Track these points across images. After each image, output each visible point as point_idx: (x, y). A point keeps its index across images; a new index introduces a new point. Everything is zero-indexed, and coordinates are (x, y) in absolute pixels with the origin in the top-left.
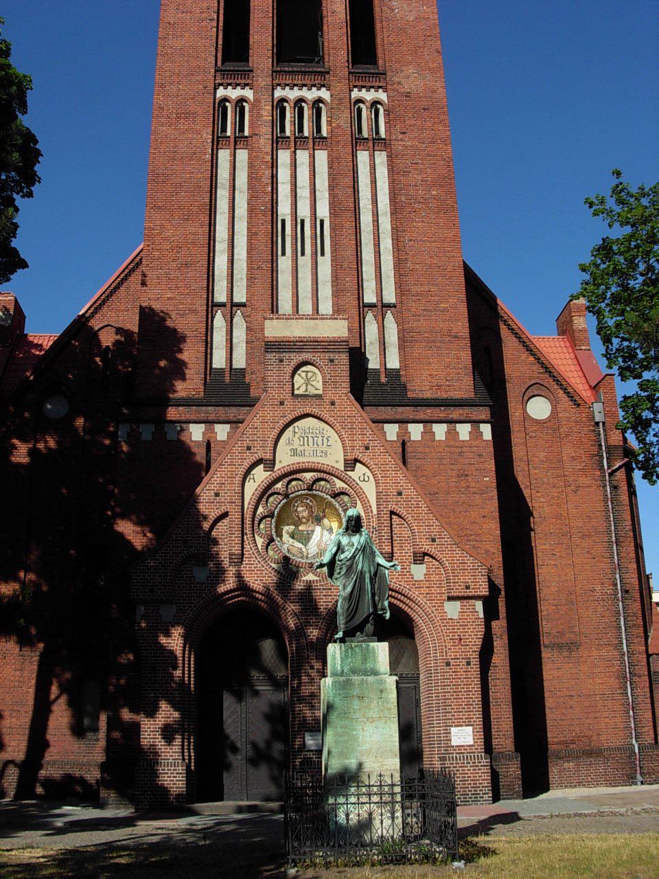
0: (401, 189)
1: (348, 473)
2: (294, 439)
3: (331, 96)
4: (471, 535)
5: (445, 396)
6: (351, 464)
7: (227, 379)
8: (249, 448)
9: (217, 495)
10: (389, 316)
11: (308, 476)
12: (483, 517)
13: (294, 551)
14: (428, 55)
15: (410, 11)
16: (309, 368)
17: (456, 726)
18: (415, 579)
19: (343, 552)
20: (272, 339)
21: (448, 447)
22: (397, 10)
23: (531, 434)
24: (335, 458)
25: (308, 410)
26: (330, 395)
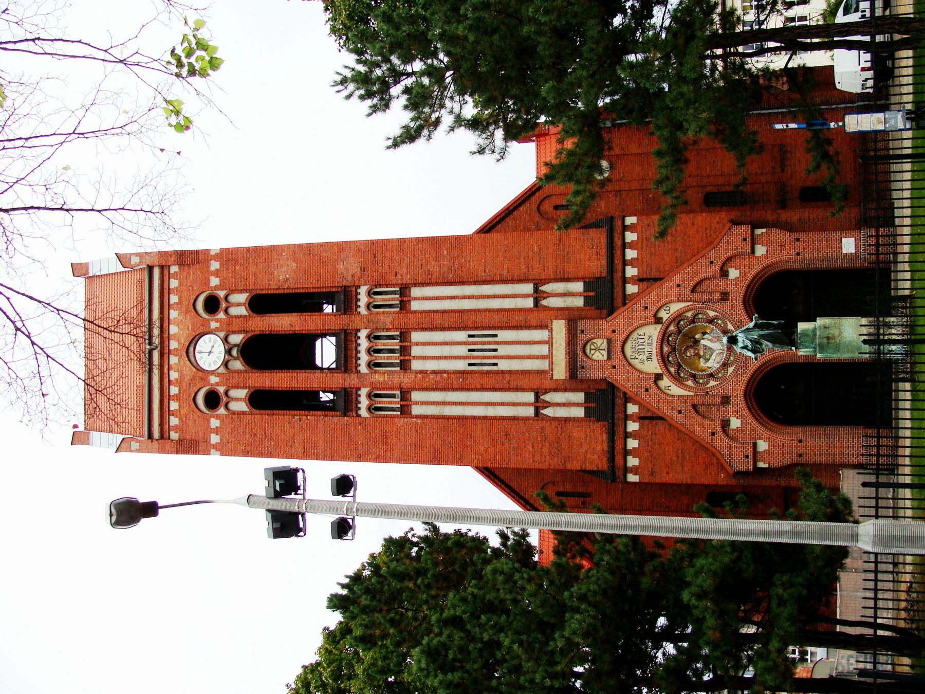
0: (443, 277)
1: (664, 321)
2: (639, 359)
3: (366, 328)
4: (707, 234)
6: (658, 321)
7: (593, 405)
8: (647, 390)
9: (680, 412)
10: (543, 288)
11: (666, 349)
12: (693, 224)
13: (718, 359)
14: (326, 252)
15: (288, 265)
16: (588, 347)
18: (738, 276)
19: (748, 346)
20: (568, 374)
21: (642, 249)
22: (287, 276)
23: (622, 175)
24: (654, 331)
25: (619, 349)
26: (608, 334)
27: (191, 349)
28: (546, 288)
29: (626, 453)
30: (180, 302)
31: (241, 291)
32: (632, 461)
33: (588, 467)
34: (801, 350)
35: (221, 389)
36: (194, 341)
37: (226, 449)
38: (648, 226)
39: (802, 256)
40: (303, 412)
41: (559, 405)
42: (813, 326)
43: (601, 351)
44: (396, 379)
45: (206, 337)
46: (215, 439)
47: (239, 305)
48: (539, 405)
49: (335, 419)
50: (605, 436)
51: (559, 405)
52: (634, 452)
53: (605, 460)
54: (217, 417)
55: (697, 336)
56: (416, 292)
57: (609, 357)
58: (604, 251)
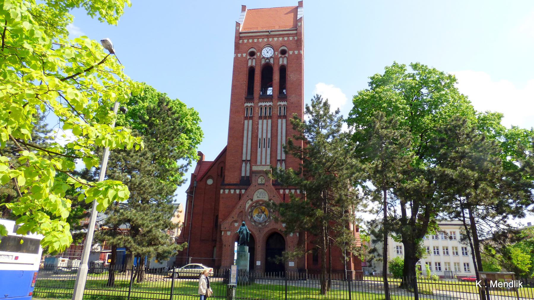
24: (266, 199)
26: (266, 184)
27: (269, 46)
28: (283, 163)
29: (230, 189)
30: (285, 41)
31: (287, 62)
32: (227, 191)
33: (226, 178)
35: (255, 57)
36: (272, 47)
37: (236, 59)
39: (288, 248)
40: (247, 85)
41: (246, 168)
44: (256, 115)
45: (273, 51)
46: (239, 55)
47: (283, 61)
48: (246, 161)
49: (244, 95)
50: (235, 183)
51: (246, 168)
52: (230, 192)
53: (227, 182)
54: (246, 56)
56: (284, 121)
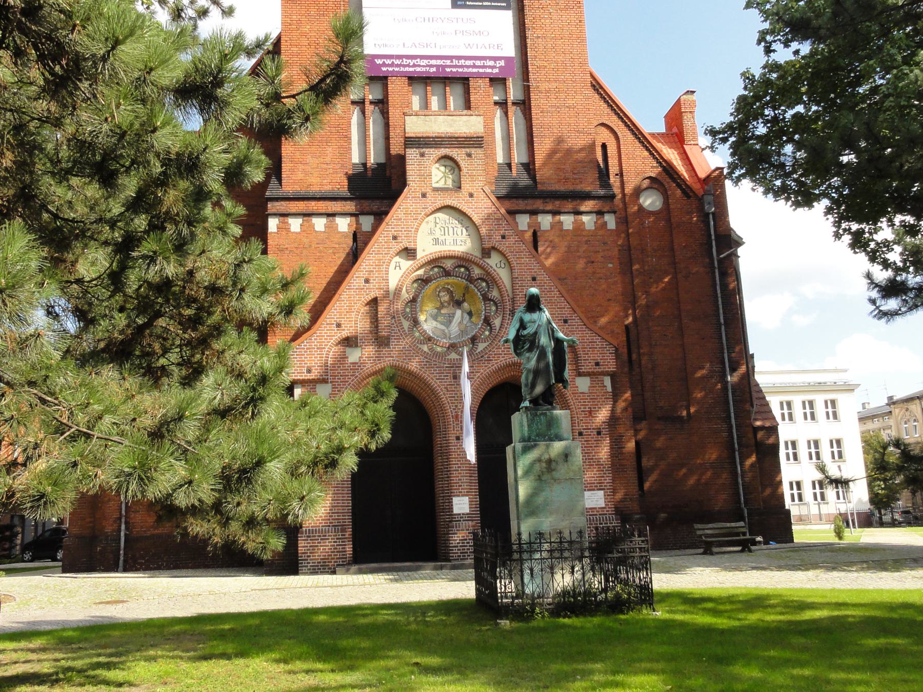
1: (485, 260)
5: (571, 188)
6: (486, 252)
8: (395, 238)
9: (367, 281)
17: (589, 490)
25: (449, 202)
34: (525, 416)
38: (605, 243)
42: (565, 436)
43: (443, 179)
50: (328, 188)
55: (465, 305)
57: (436, 190)
58: (569, 187)
